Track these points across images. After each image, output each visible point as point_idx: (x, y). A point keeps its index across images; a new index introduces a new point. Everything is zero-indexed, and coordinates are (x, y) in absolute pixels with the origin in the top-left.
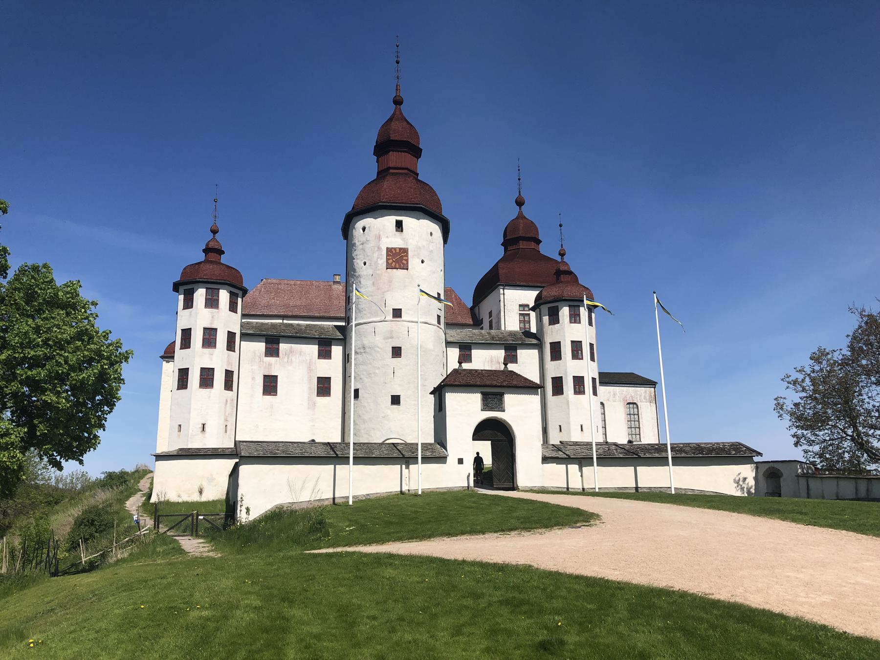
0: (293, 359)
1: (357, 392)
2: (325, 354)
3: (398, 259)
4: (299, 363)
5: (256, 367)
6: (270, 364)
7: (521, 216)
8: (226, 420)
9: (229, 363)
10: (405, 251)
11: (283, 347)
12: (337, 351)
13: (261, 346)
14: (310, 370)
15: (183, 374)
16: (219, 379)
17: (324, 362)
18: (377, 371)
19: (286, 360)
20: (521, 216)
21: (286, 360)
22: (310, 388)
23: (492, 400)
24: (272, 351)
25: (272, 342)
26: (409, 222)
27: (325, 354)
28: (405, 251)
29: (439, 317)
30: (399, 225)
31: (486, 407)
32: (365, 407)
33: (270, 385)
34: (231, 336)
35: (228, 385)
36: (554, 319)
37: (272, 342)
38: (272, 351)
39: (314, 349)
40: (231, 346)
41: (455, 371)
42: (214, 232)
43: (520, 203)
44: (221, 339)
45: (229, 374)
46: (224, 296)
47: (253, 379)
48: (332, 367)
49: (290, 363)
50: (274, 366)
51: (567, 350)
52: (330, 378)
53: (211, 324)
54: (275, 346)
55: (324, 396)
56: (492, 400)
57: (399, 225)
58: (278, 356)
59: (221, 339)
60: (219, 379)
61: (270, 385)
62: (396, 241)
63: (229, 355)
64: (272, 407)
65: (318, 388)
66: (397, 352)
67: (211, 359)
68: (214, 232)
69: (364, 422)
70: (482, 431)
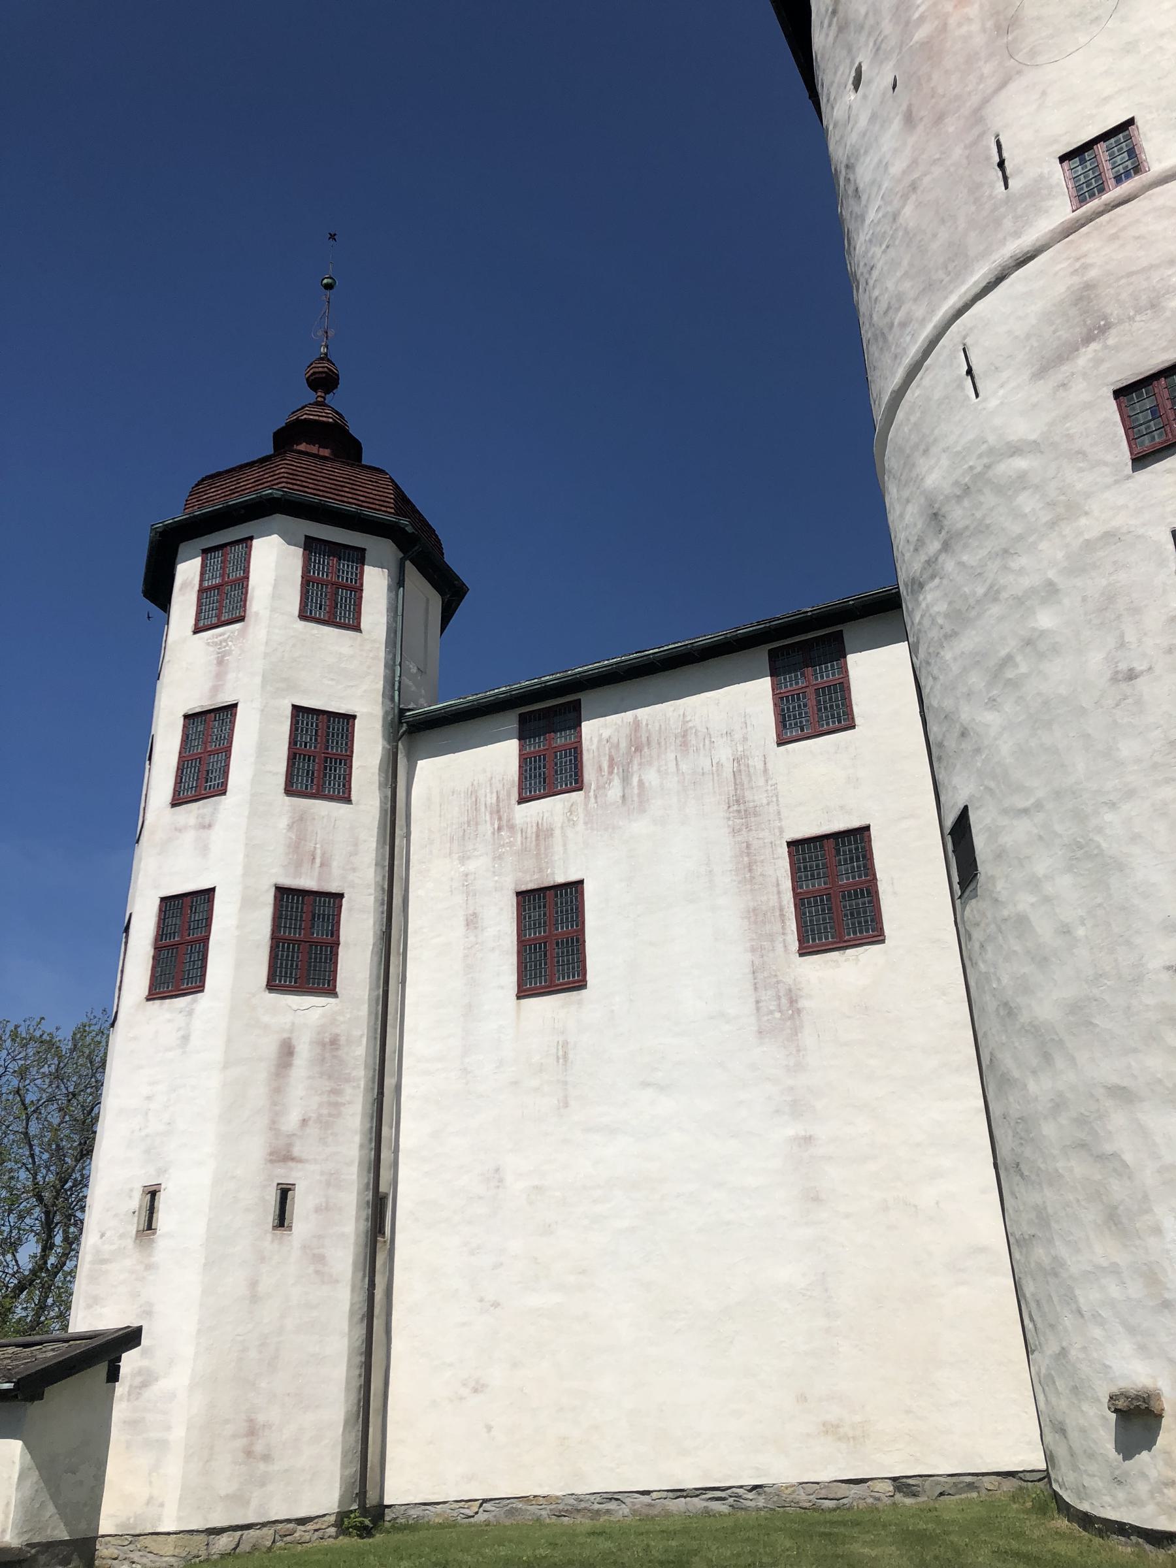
0: (651, 777)
2: (815, 709)
5: (479, 864)
6: (543, 834)
8: (282, 1155)
9: (299, 851)
13: (499, 758)
14: (742, 811)
17: (818, 753)
18: (1045, 619)
19: (614, 792)
21: (614, 792)
22: (756, 916)
24: (551, 771)
25: (547, 724)
32: (1022, 923)
33: (551, 940)
37: (547, 724)
39: (751, 699)
42: (324, 382)
46: (274, 562)
47: (472, 922)
49: (636, 801)
50: (572, 838)
52: (863, 832)
53: (215, 689)
54: (561, 740)
55: (841, 944)
58: (577, 784)
60: (239, 940)
61: (551, 940)
63: (299, 822)
64: (564, 1057)
65: (800, 901)
67: (204, 849)
68: (324, 382)
69: (1047, 1045)
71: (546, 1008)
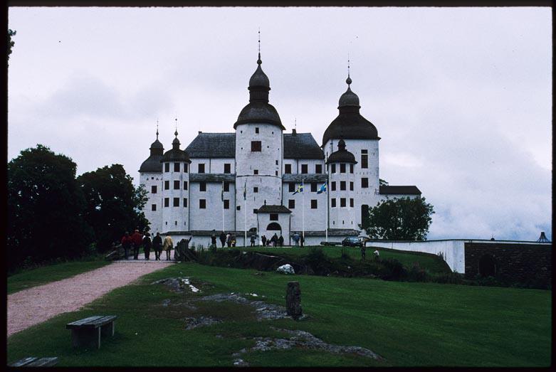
1: (239, 208)
2: (226, 189)
3: (256, 146)
4: (215, 191)
7: (349, 91)
10: (259, 143)
11: (208, 187)
12: (231, 187)
15: (167, 200)
16: (181, 202)
20: (349, 91)
23: (274, 217)
24: (203, 189)
26: (262, 128)
27: (226, 189)
28: (259, 143)
29: (277, 172)
30: (257, 131)
31: (271, 219)
33: (203, 204)
34: (186, 183)
35: (185, 205)
36: (334, 171)
38: (203, 189)
40: (185, 188)
41: (263, 206)
43: (349, 82)
44: (182, 186)
45: (185, 200)
48: (227, 195)
51: (338, 186)
56: (274, 217)
57: (257, 131)
59: (182, 186)
60: (181, 202)
61: (203, 204)
62: (257, 138)
66: (256, 190)
70: (271, 227)
71: (202, 209)
